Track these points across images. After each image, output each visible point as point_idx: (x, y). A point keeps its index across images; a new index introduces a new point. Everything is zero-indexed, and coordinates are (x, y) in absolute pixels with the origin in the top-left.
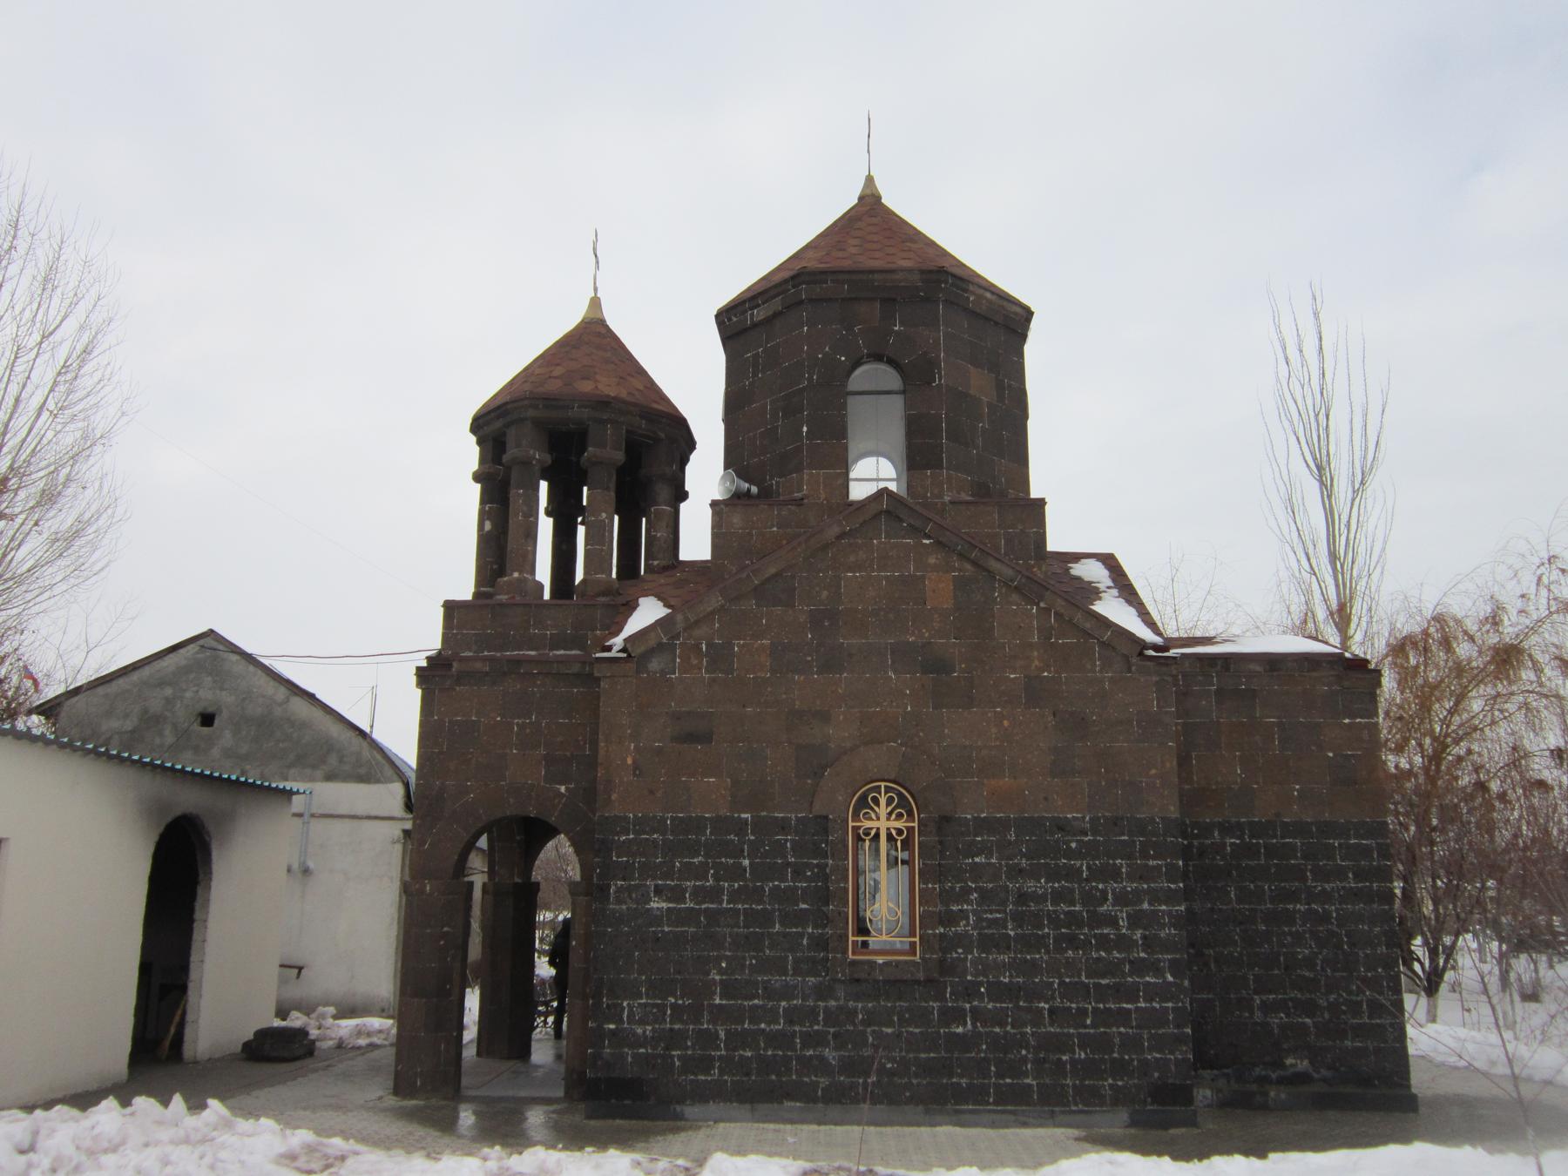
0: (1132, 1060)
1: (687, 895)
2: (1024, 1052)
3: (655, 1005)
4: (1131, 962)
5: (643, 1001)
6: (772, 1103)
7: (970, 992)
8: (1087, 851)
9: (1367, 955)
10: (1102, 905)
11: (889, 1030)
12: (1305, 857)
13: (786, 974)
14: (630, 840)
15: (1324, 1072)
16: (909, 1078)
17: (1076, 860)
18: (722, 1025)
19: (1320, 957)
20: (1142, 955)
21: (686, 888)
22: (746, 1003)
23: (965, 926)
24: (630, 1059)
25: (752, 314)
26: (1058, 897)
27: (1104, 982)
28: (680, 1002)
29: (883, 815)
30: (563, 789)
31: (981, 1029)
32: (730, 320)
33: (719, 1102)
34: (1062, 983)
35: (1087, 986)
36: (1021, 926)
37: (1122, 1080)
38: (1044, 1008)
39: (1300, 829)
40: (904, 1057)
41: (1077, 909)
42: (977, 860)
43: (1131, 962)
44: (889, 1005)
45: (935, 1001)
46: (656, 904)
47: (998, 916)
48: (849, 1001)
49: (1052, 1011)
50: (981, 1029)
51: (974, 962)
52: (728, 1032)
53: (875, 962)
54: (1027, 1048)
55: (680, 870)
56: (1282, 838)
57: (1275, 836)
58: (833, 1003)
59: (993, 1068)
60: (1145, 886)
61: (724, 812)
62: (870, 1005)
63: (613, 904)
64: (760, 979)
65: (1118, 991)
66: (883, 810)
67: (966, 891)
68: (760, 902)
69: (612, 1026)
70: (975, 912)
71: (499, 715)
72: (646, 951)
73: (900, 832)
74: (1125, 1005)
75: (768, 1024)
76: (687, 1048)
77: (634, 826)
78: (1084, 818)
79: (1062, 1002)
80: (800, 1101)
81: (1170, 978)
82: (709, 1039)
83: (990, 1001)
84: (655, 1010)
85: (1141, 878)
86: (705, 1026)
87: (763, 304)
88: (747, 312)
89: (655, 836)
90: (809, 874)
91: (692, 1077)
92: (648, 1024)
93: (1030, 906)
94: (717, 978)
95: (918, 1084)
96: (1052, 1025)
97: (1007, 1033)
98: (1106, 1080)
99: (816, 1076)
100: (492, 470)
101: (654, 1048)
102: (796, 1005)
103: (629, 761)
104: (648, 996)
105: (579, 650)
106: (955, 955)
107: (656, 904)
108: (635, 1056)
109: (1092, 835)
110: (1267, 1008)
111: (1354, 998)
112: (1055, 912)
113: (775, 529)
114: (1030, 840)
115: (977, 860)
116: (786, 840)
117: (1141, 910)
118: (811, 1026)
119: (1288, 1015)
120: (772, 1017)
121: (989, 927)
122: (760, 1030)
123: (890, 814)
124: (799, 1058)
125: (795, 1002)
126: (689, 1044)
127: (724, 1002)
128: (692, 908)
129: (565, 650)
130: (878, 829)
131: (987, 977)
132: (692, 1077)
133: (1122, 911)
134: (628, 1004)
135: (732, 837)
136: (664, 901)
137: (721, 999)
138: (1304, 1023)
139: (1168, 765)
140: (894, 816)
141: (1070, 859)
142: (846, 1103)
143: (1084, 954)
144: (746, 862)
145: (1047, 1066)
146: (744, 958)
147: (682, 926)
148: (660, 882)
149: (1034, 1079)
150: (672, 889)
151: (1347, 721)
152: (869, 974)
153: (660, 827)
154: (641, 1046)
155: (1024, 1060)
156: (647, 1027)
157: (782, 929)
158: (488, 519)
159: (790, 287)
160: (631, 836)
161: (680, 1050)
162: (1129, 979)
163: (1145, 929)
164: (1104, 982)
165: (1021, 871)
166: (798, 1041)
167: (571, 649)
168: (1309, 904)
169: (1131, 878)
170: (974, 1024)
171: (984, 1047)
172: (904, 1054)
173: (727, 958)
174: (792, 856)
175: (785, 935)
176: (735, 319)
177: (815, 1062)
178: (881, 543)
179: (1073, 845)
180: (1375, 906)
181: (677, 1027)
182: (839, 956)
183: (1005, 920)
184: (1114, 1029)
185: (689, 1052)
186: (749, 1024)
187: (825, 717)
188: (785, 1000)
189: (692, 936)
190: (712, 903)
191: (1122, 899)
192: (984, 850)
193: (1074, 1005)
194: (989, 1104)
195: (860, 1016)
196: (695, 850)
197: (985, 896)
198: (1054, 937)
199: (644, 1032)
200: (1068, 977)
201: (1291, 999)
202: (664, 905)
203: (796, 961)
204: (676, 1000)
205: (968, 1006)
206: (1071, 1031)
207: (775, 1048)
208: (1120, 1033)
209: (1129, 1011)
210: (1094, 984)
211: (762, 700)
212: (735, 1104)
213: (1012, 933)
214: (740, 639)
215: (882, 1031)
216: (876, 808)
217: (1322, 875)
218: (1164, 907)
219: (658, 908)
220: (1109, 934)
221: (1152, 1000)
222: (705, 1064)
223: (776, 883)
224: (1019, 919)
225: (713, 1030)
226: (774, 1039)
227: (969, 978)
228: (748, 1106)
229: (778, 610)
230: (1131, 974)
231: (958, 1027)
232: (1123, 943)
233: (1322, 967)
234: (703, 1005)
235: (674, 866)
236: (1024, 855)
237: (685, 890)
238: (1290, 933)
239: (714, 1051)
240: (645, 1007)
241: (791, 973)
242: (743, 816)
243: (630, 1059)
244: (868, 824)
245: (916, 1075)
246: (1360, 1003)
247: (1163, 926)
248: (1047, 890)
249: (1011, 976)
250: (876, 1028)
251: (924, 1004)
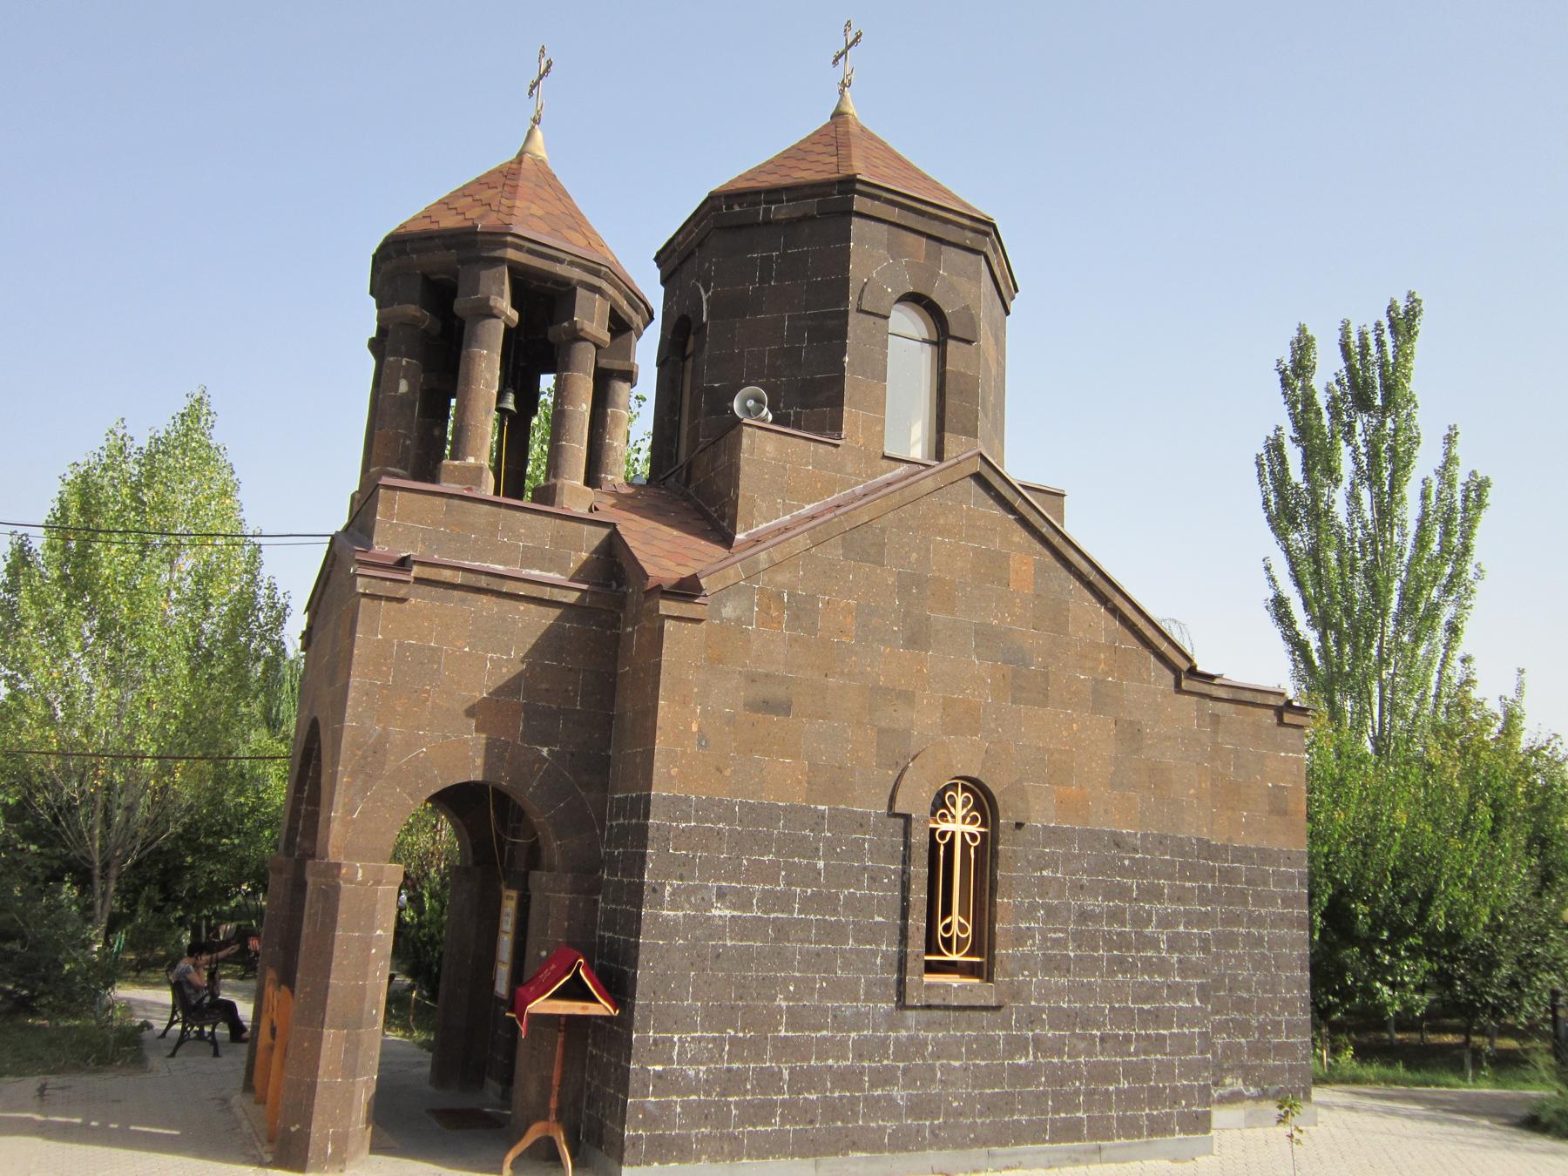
0: (1165, 1087)
1: (755, 902)
2: (1077, 1084)
3: (709, 1040)
4: (1169, 986)
5: (699, 1034)
6: (837, 1154)
7: (1032, 1019)
8: (1138, 869)
9: (1287, 977)
10: (1147, 927)
11: (957, 1064)
12: (1248, 882)
13: (857, 1000)
14: (691, 829)
15: (1252, 1090)
16: (974, 1117)
17: (1129, 878)
18: (786, 1062)
19: (1255, 979)
20: (1177, 979)
21: (754, 892)
22: (813, 1035)
23: (1031, 946)
24: (679, 1110)
25: (767, 211)
26: (1115, 916)
27: (1146, 1007)
28: (741, 1035)
29: (959, 818)
30: (545, 751)
31: (1041, 1060)
32: (729, 207)
33: (779, 1158)
34: (1112, 1009)
35: (1132, 1011)
36: (1079, 947)
37: (1157, 1109)
38: (1096, 1036)
39: (1244, 854)
40: (970, 1094)
41: (1127, 930)
42: (1045, 873)
43: (1169, 986)
44: (958, 1034)
45: (1000, 1030)
46: (720, 912)
47: (1062, 935)
48: (919, 1030)
49: (1102, 1039)
50: (1041, 1060)
51: (1039, 986)
52: (792, 1071)
53: (951, 986)
54: (1080, 1080)
55: (747, 870)
56: (1233, 862)
57: (1226, 861)
58: (904, 1033)
59: (1050, 1103)
60: (1182, 908)
61: (799, 801)
62: (940, 1035)
63: (668, 910)
64: (829, 1005)
65: (1157, 1016)
66: (959, 812)
67: (1033, 908)
68: (835, 912)
69: (659, 1068)
70: (1040, 930)
71: (468, 644)
72: (704, 970)
73: (973, 837)
74: (1162, 1032)
75: (837, 1059)
76: (746, 1091)
77: (697, 811)
78: (1136, 834)
79: (1111, 1029)
80: (864, 1150)
81: (1198, 1004)
82: (769, 1080)
83: (1051, 1027)
84: (710, 1046)
85: (1179, 899)
86: (768, 1064)
87: (788, 201)
88: (760, 204)
89: (721, 825)
90: (886, 881)
91: (751, 1129)
92: (702, 1063)
93: (1088, 926)
94: (784, 1004)
95: (983, 1123)
96: (1101, 1054)
97: (1063, 1062)
98: (1144, 1110)
99: (882, 1120)
100: (418, 314)
101: (708, 1094)
102: (865, 1036)
103: (694, 728)
104: (704, 1029)
105: (559, 572)
106: (1021, 978)
107: (720, 912)
108: (685, 1105)
109: (1142, 853)
111: (1277, 1018)
112: (1109, 932)
113: (810, 468)
114: (1091, 854)
115: (1045, 873)
116: (864, 840)
117: (1178, 933)
118: (880, 1061)
119: (1229, 1037)
120: (840, 1049)
121: (1052, 948)
122: (826, 1066)
123: (964, 818)
124: (866, 1099)
125: (865, 1033)
126: (749, 1087)
127: (790, 1034)
128: (760, 917)
129: (541, 570)
130: (953, 833)
131: (1049, 1002)
132: (751, 1129)
133: (1163, 933)
134: (680, 1039)
135: (807, 832)
136: (728, 908)
137: (786, 1031)
138: (1239, 1043)
139: (1203, 785)
140: (968, 820)
141: (1124, 877)
142: (913, 1150)
143: (1131, 978)
144: (821, 864)
145: (1097, 1097)
146: (814, 980)
147: (749, 940)
148: (724, 884)
149: (1085, 1112)
150: (737, 892)
151: (1282, 754)
152: (944, 1000)
153: (727, 814)
154: (693, 1092)
155: (1077, 1092)
156: (701, 1068)
157: (856, 946)
158: (405, 377)
159: (836, 192)
160: (693, 824)
161: (738, 1095)
162: (1167, 1004)
163: (1181, 953)
164: (1146, 1007)
165: (1082, 887)
166: (867, 1079)
167: (550, 571)
168: (1249, 928)
169: (1171, 900)
170: (1036, 1057)
171: (1043, 1079)
172: (969, 1090)
173: (796, 980)
174: (869, 860)
175: (858, 952)
176: (737, 208)
177: (883, 1103)
178: (969, 508)
179: (1127, 862)
180: (1295, 931)
181: (735, 1066)
182: (916, 978)
183: (1066, 940)
184: (1152, 1057)
185: (748, 1098)
186: (817, 1059)
187: (908, 698)
188: (854, 1031)
189: (758, 953)
190: (783, 912)
191: (1165, 922)
192: (1052, 863)
193: (1121, 1032)
194: (1044, 1141)
195: (930, 1048)
196: (766, 846)
197: (1052, 912)
198: (1108, 960)
199: (697, 1074)
200: (1118, 1002)
201: (1232, 1020)
202: (728, 913)
203: (869, 984)
204: (736, 1032)
205: (1030, 1034)
206: (1118, 1059)
207: (842, 1089)
208: (1156, 1060)
209: (1164, 1036)
210: (1139, 1009)
211: (846, 671)
212: (796, 1159)
213: (1072, 954)
214: (825, 594)
215: (950, 1065)
216: (952, 809)
217: (1260, 900)
218: (1195, 931)
219: (720, 916)
220: (1151, 957)
221: (1183, 1025)
222: (762, 1112)
223: (852, 890)
224: (1080, 939)
225: (776, 1069)
226: (846, 1078)
227: (1033, 1003)
228: (811, 1160)
229: (867, 567)
230: (1169, 997)
231: (1021, 1058)
232: (1162, 967)
233: (1256, 989)
234: (766, 1038)
235: (741, 864)
236: (1085, 871)
237: (752, 894)
238: (1233, 956)
239: (775, 1095)
240: (700, 1042)
241: (862, 997)
242: (820, 807)
243: (679, 1110)
244: (943, 827)
245: (981, 1114)
246: (1280, 1023)
247: (1194, 949)
248: (1103, 909)
249: (1069, 1001)
250: (945, 1061)
251: (991, 1033)
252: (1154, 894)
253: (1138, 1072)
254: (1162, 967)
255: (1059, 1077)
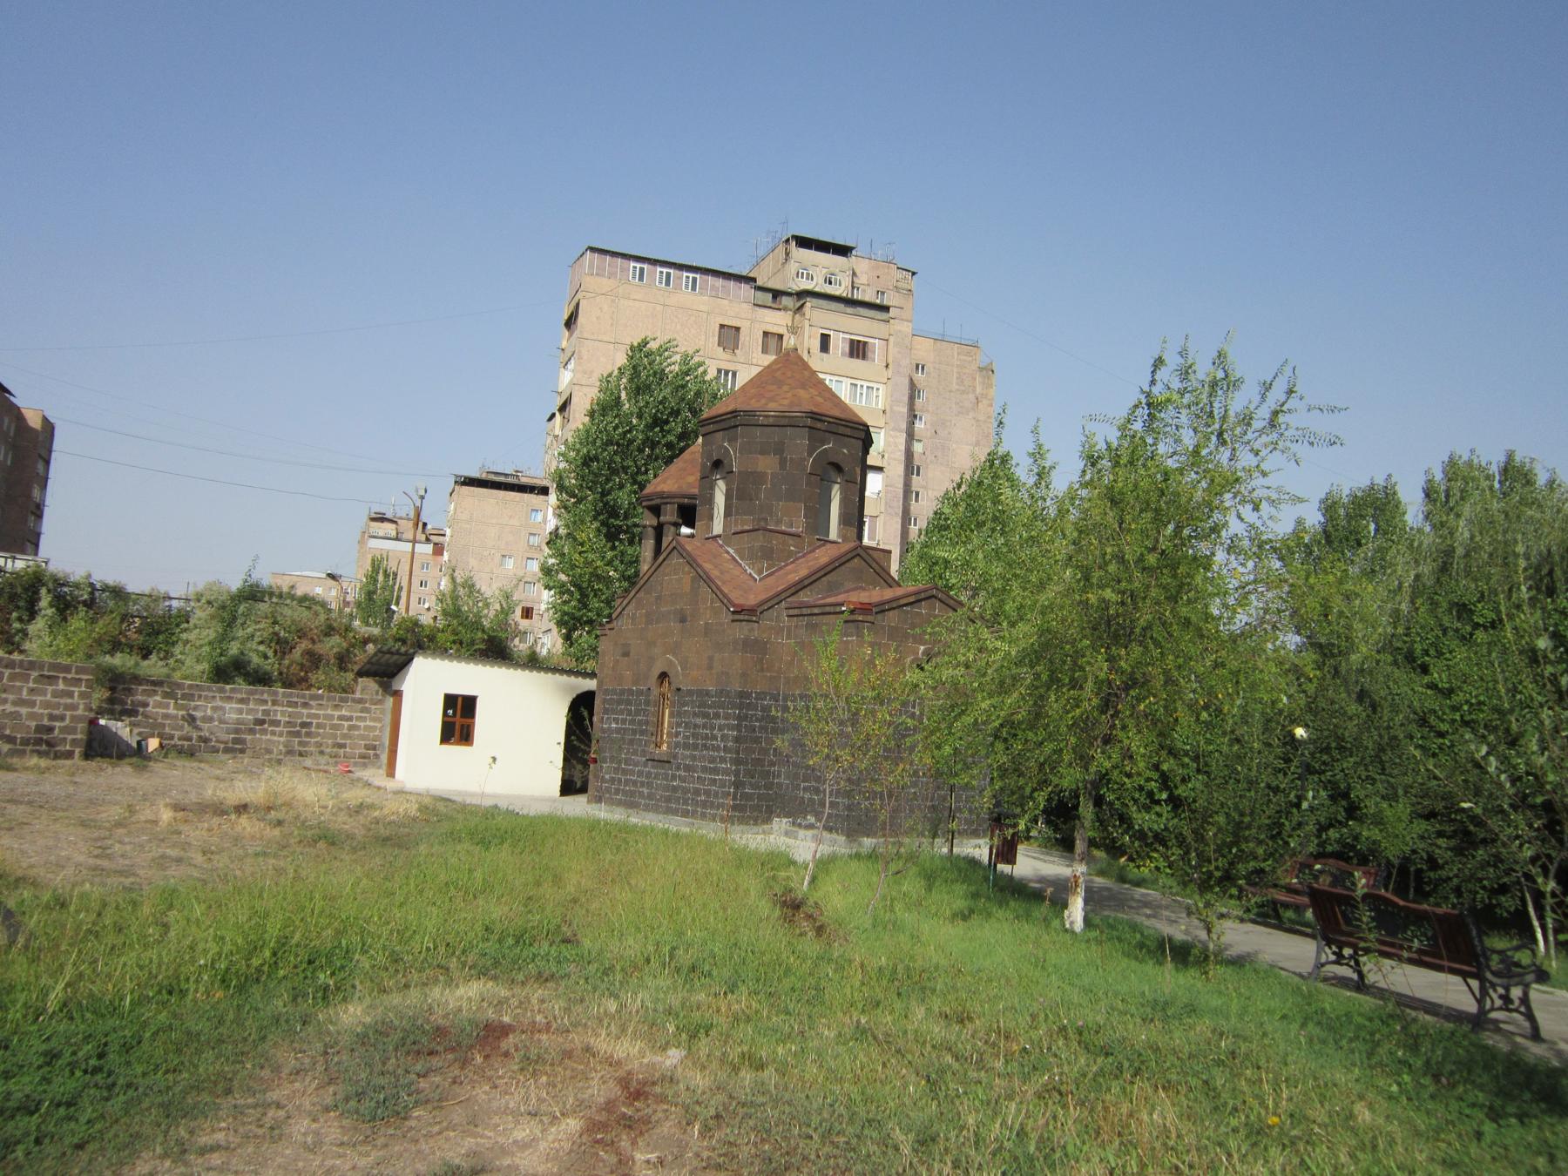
7: (678, 768)
110: (805, 789)
222: (617, 791)
224: (694, 736)
232: (717, 749)
252: (717, 716)
253: (707, 793)
254: (717, 749)
255: (685, 791)
